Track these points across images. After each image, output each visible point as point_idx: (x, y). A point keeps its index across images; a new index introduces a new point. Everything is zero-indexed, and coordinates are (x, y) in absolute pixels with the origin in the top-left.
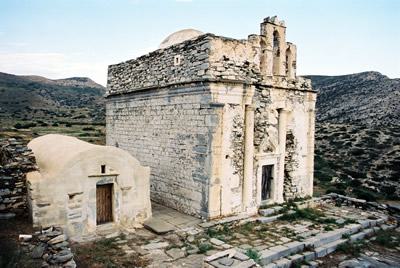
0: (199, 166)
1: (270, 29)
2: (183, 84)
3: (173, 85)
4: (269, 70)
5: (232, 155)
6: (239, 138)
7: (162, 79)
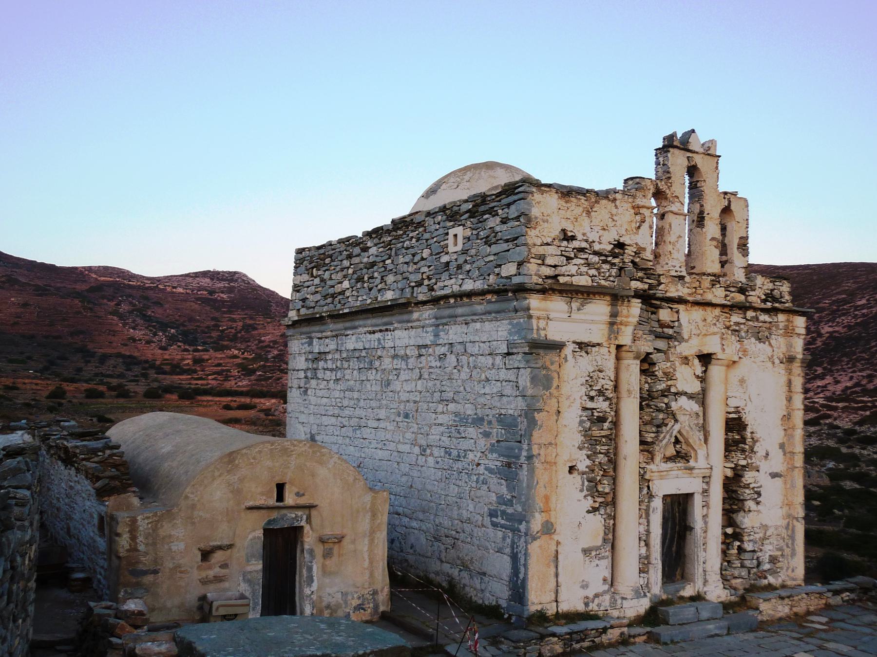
0: (504, 490)
1: (678, 161)
2: (470, 294)
3: (446, 297)
4: (674, 260)
5: (583, 464)
6: (601, 431)
7: (420, 284)
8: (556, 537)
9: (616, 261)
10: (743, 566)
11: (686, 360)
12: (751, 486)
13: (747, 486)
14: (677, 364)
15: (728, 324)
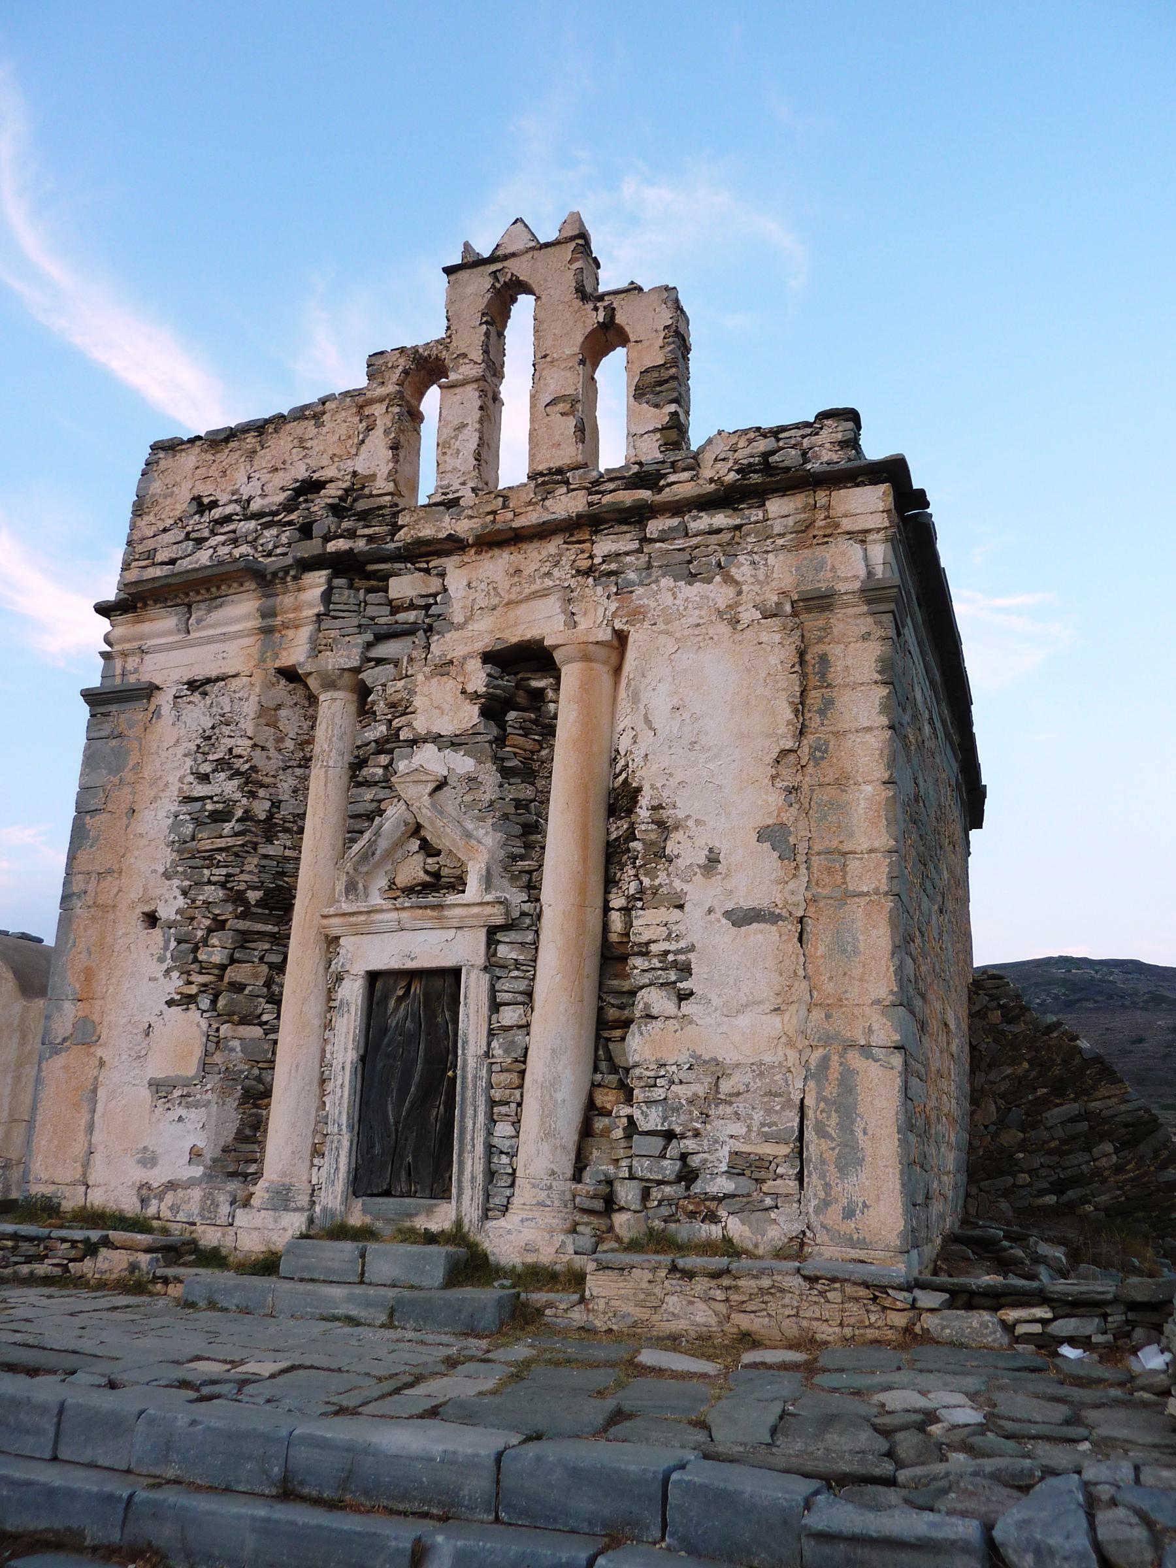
8: (99, 1052)
9: (292, 517)
11: (445, 667)
14: (420, 677)
15: (585, 564)
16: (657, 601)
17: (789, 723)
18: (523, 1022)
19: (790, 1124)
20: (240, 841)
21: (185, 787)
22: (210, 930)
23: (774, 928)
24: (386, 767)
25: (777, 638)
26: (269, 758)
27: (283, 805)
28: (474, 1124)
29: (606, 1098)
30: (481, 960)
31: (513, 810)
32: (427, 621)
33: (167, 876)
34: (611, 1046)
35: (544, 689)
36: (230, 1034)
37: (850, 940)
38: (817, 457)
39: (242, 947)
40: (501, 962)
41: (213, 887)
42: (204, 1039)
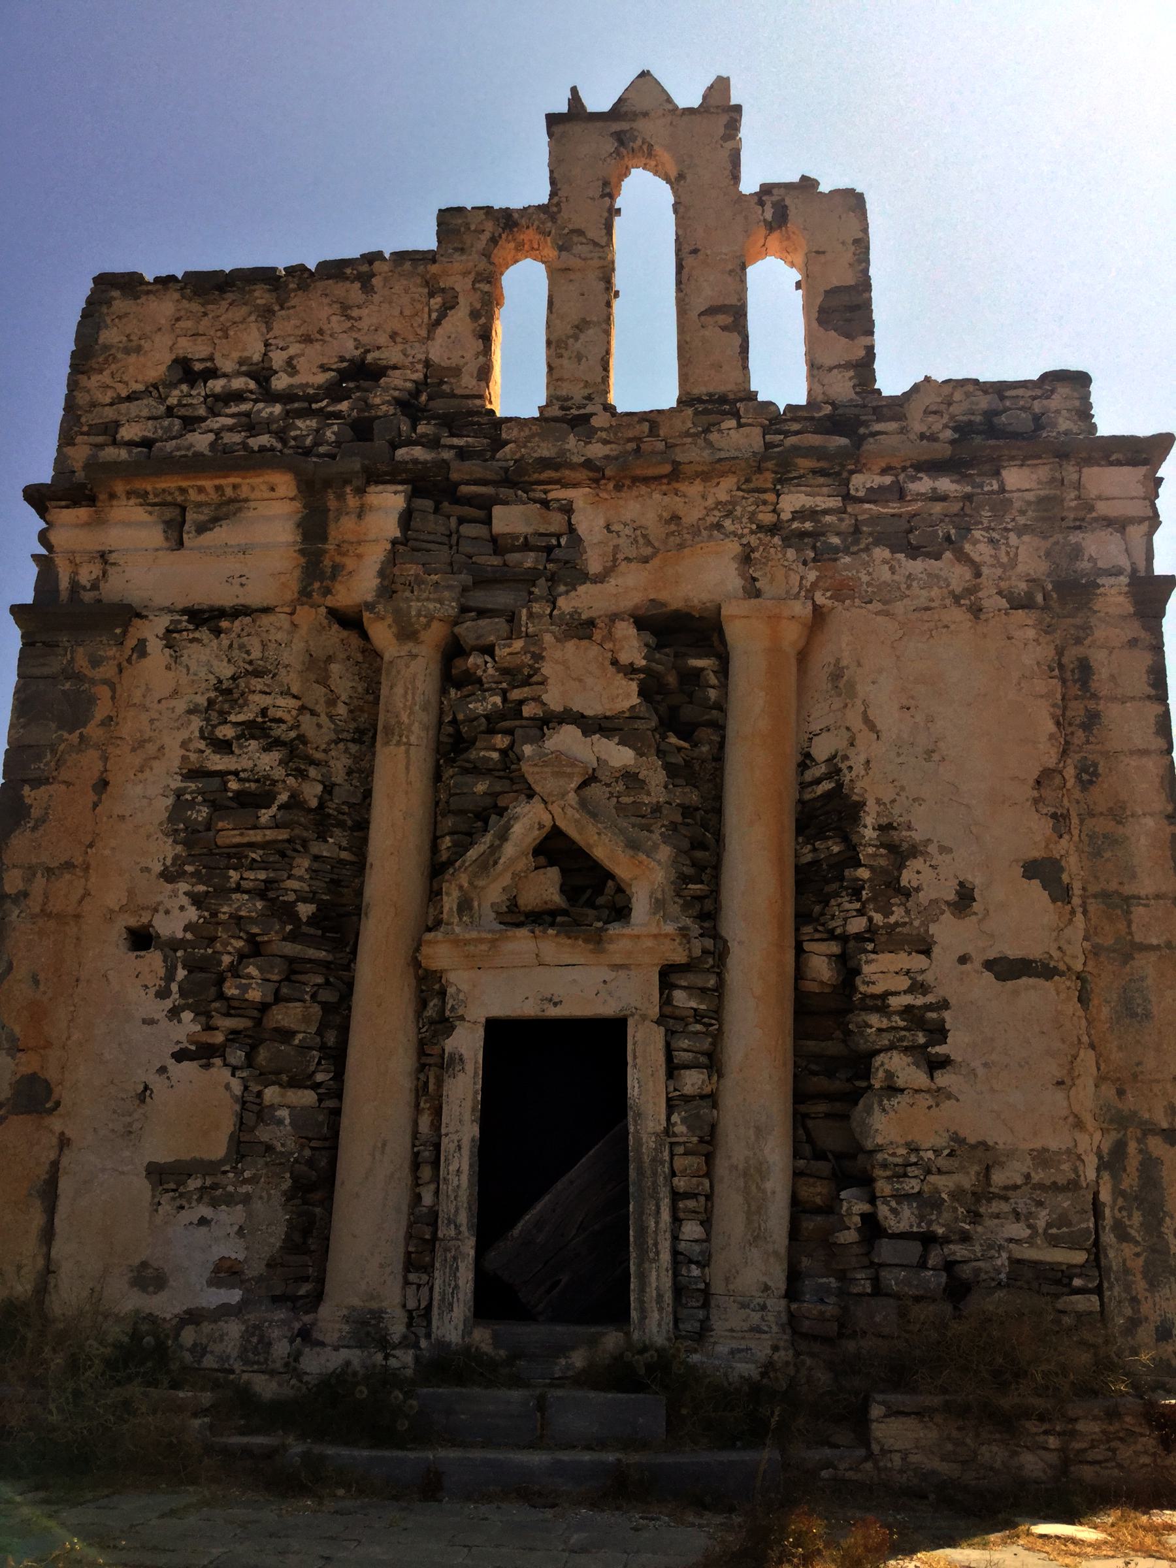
5: (175, 919)
8: (56, 1124)
9: (344, 406)
10: (878, 1290)
11: (582, 628)
12: (895, 1002)
13: (880, 1003)
14: (548, 638)
15: (767, 518)
16: (869, 574)
17: (1052, 737)
18: (707, 1090)
19: (1084, 1225)
20: (283, 835)
21: (193, 757)
22: (242, 956)
23: (1048, 984)
24: (504, 752)
25: (1031, 633)
26: (319, 726)
27: (336, 790)
28: (657, 1223)
29: (812, 1190)
30: (655, 1012)
31: (679, 819)
32: (550, 566)
33: (169, 876)
34: (810, 1124)
35: (703, 669)
36: (276, 1101)
37: (1139, 1001)
38: (1054, 425)
39: (287, 979)
40: (677, 1012)
41: (246, 897)
42: (238, 1107)
